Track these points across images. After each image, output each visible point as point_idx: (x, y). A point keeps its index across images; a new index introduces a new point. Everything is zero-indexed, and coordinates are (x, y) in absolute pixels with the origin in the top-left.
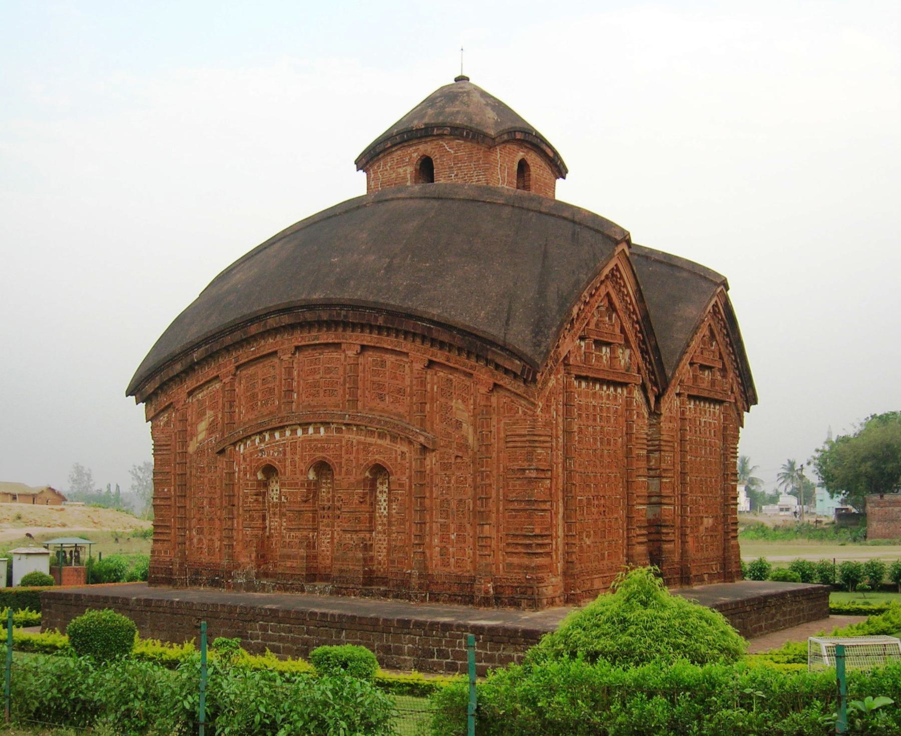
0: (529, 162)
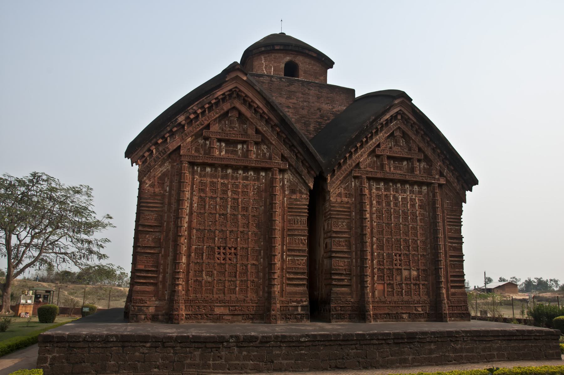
0: (297, 62)
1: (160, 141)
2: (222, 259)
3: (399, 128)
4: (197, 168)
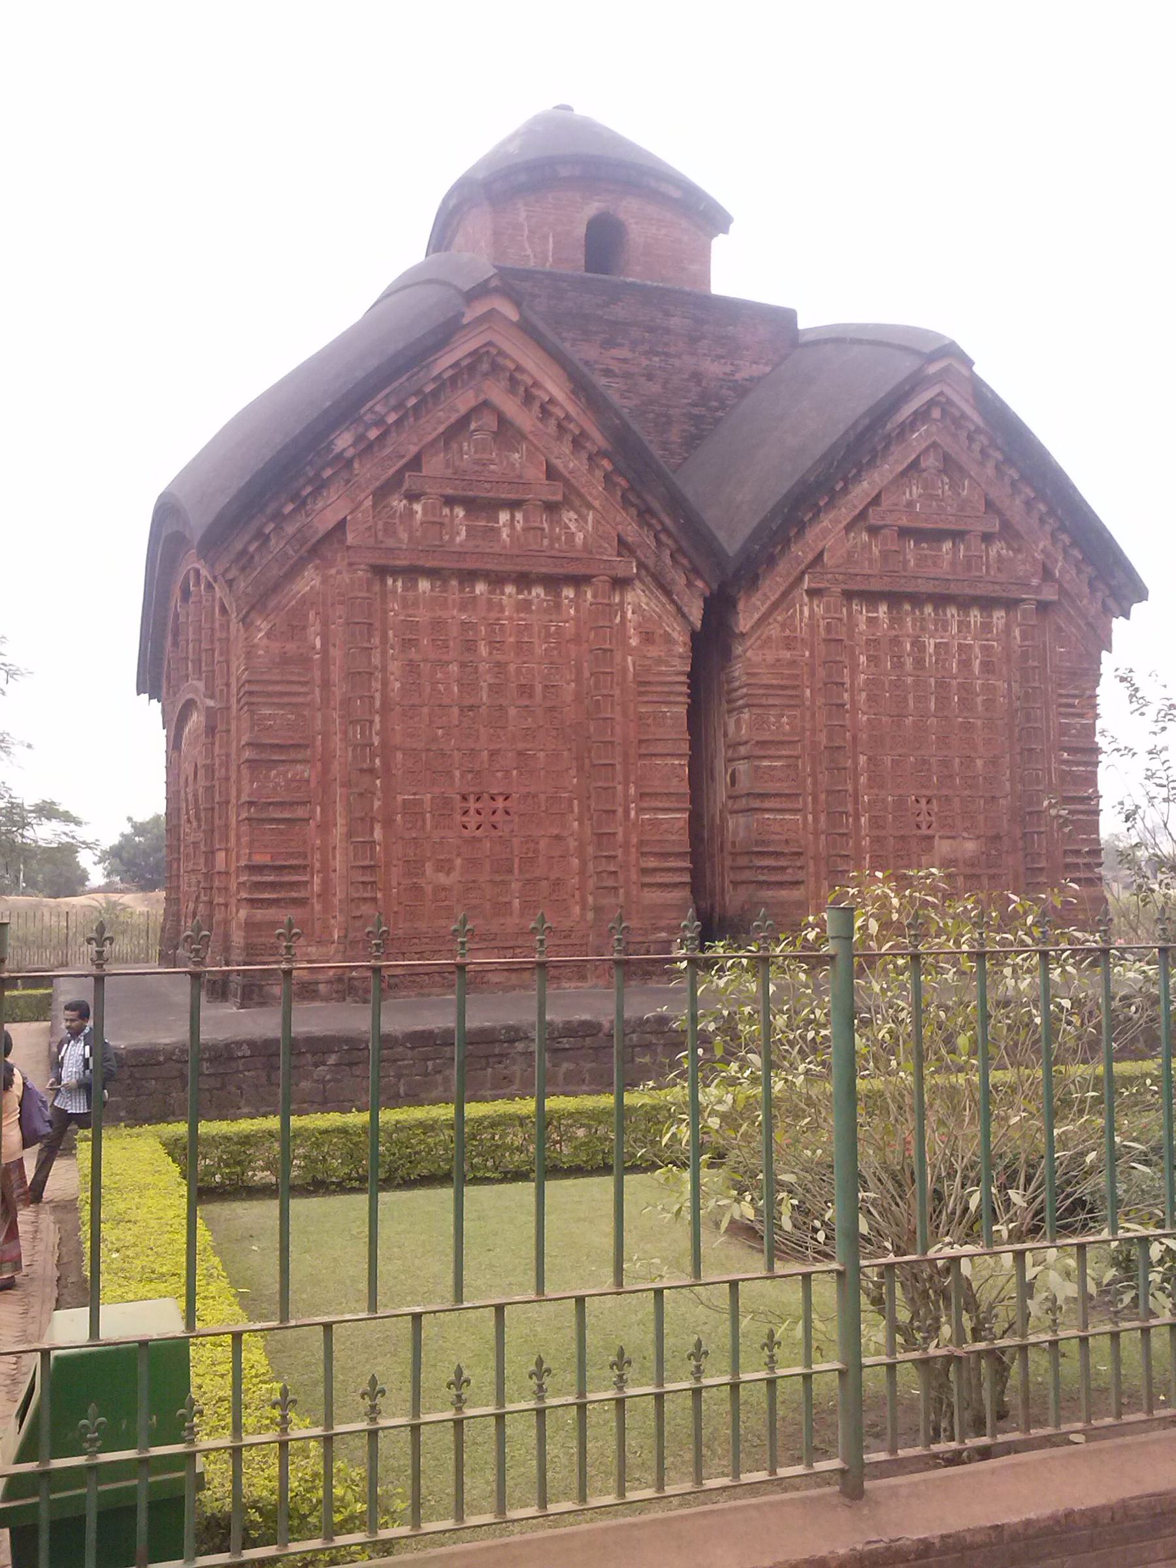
0: (622, 216)
1: (289, 508)
2: (472, 826)
3: (934, 445)
4: (394, 581)
